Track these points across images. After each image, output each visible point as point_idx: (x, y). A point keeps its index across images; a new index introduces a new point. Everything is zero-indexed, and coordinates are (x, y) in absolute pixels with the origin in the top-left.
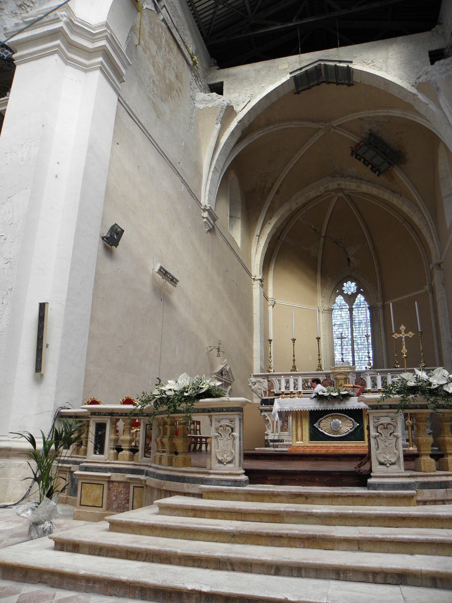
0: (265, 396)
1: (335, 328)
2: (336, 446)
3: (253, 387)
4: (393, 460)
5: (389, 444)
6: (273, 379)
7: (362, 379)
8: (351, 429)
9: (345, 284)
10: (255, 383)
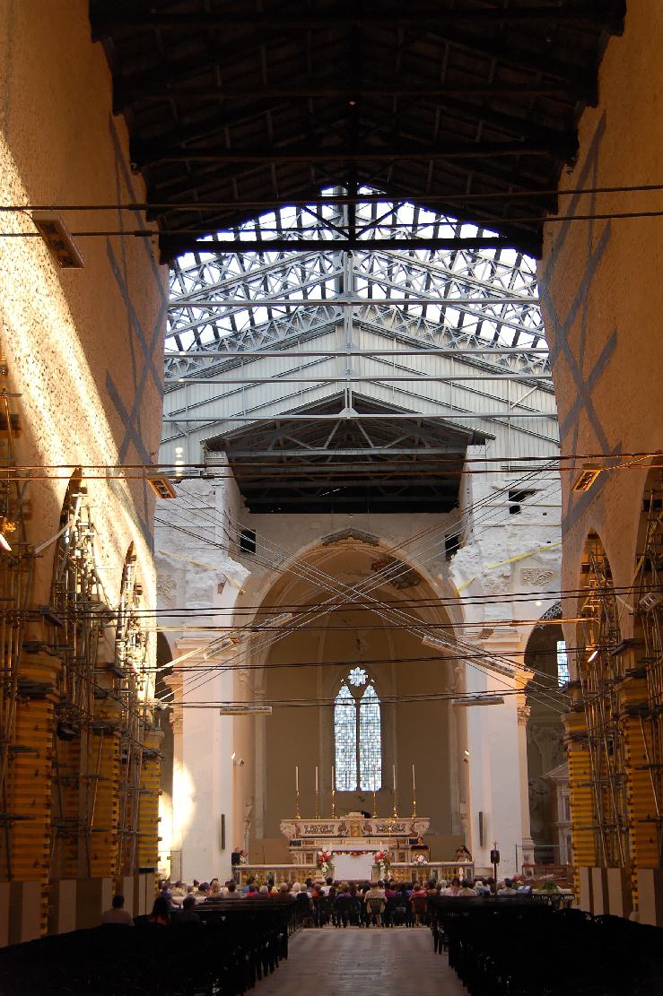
1: (337, 729)
9: (352, 671)
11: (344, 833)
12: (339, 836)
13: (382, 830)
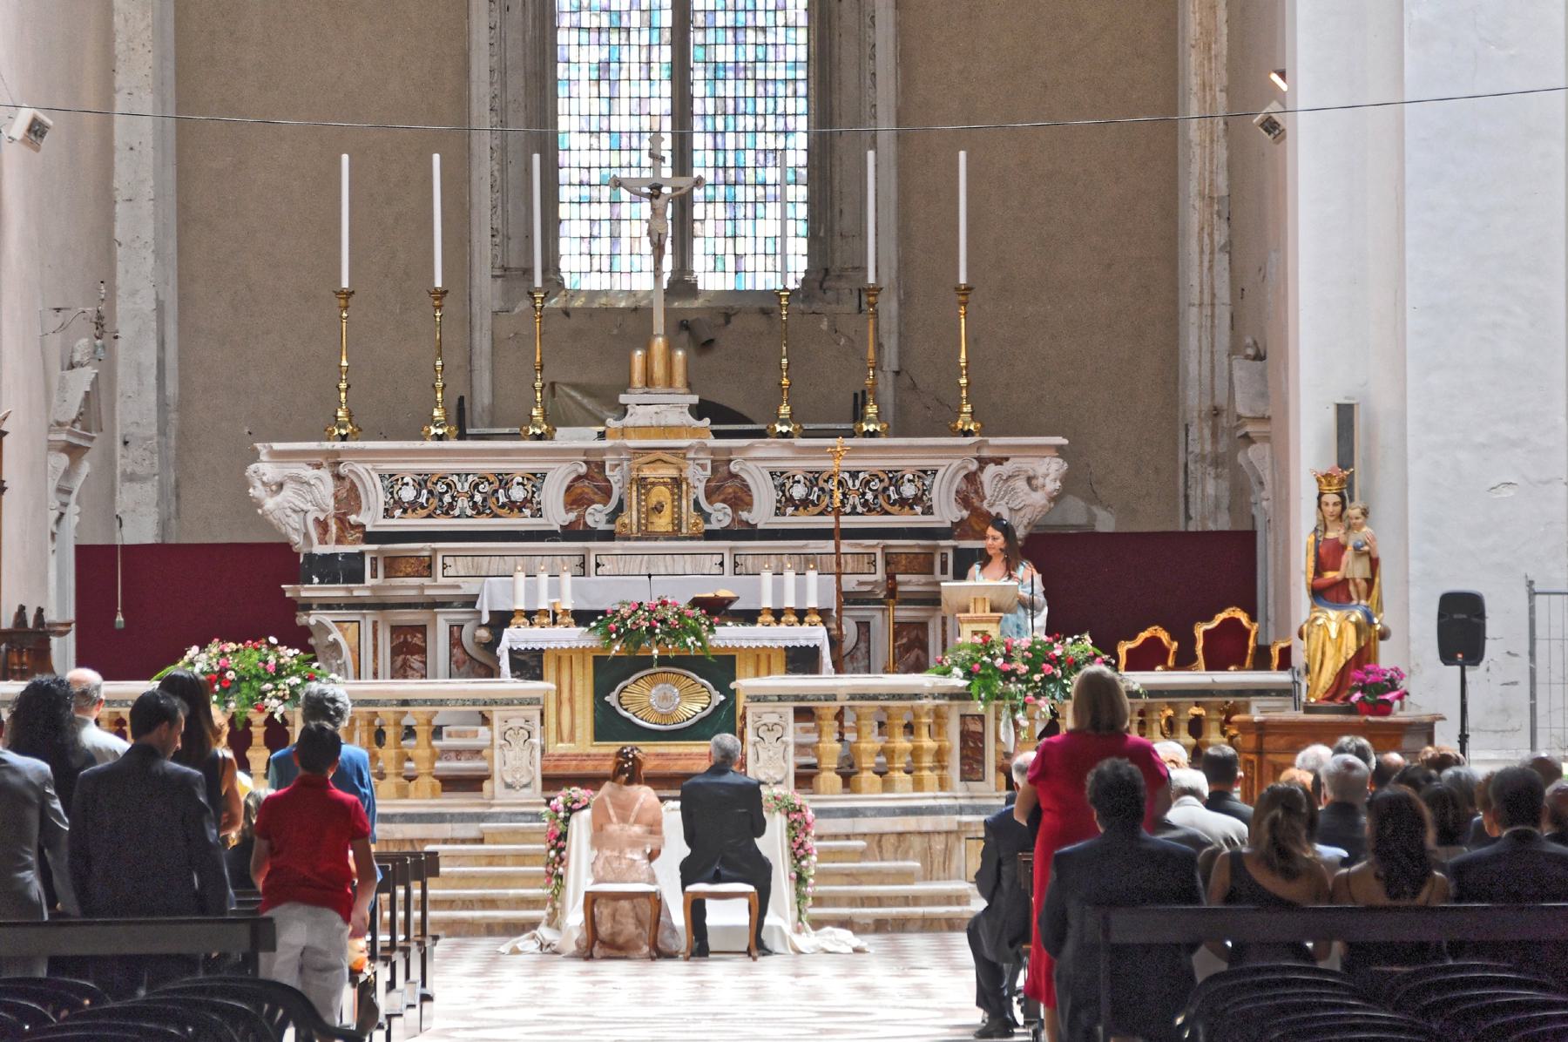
0: (323, 541)
2: (663, 755)
3: (270, 503)
4: (779, 778)
5: (775, 754)
6: (360, 468)
7: (735, 476)
8: (703, 709)
10: (281, 486)
11: (596, 517)
12: (570, 533)
13: (805, 503)
